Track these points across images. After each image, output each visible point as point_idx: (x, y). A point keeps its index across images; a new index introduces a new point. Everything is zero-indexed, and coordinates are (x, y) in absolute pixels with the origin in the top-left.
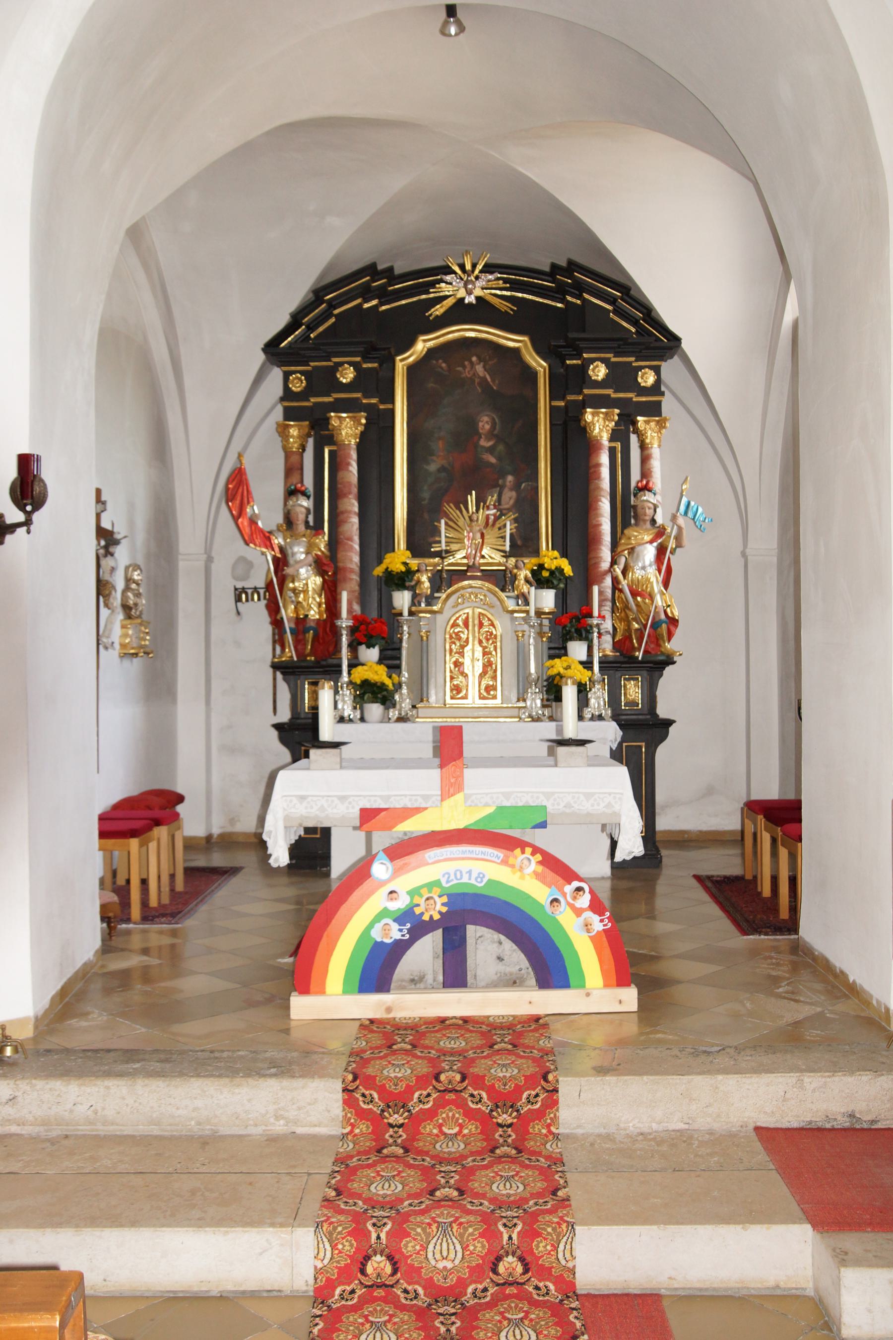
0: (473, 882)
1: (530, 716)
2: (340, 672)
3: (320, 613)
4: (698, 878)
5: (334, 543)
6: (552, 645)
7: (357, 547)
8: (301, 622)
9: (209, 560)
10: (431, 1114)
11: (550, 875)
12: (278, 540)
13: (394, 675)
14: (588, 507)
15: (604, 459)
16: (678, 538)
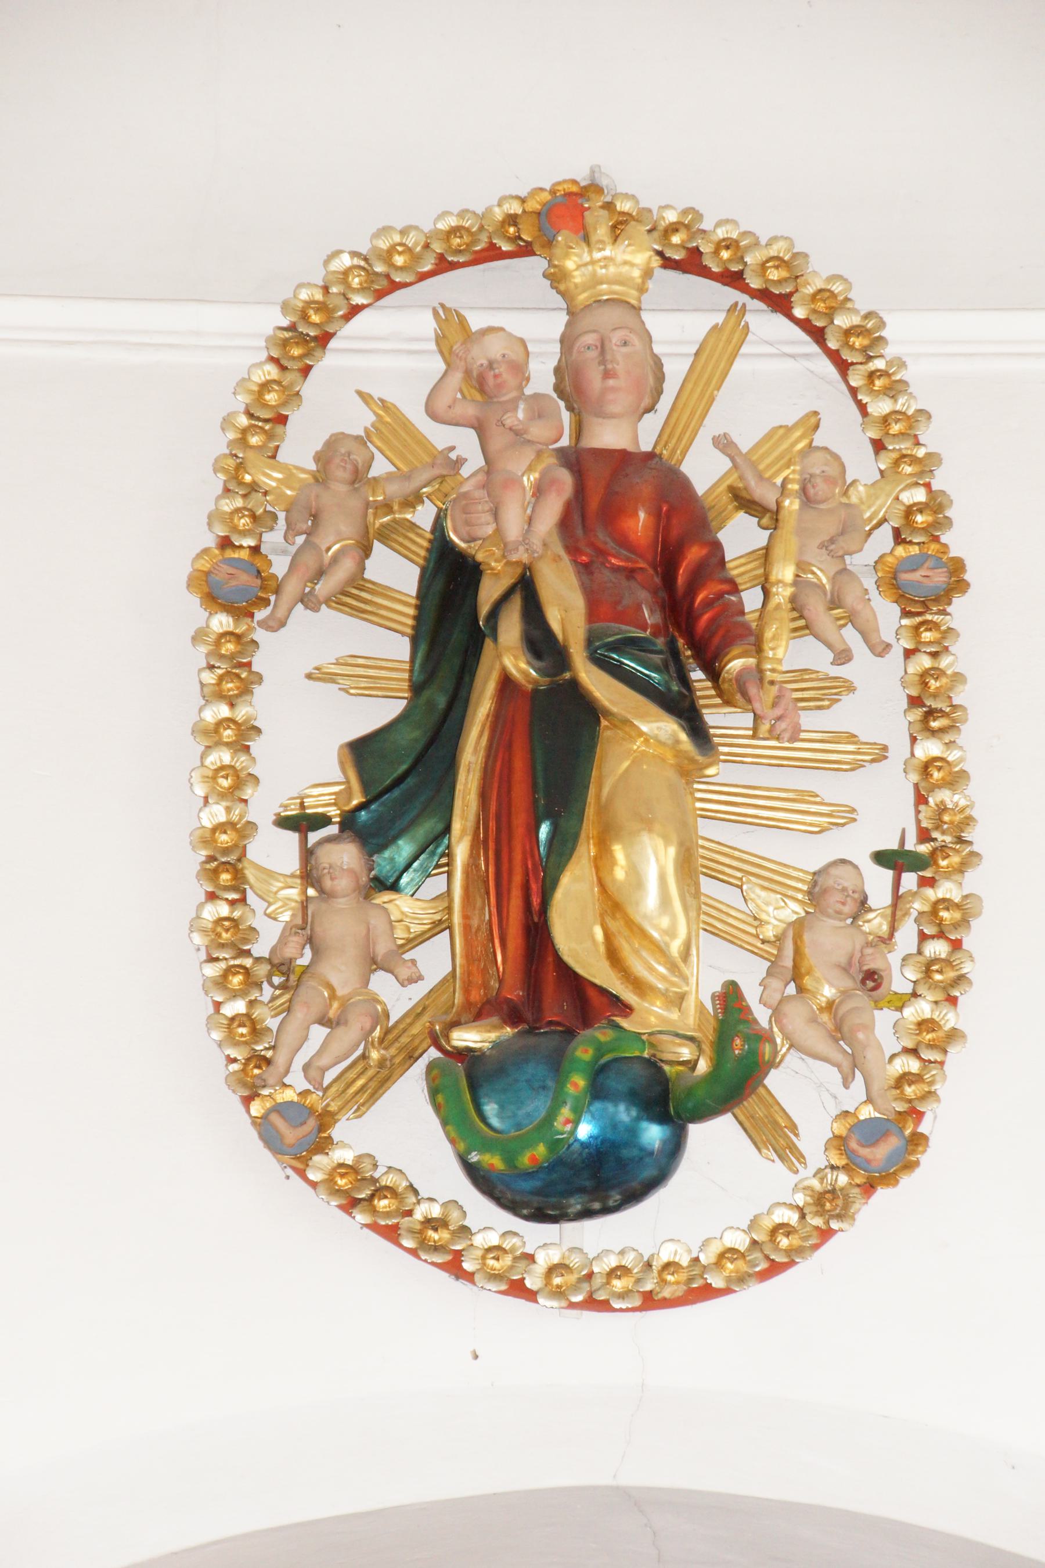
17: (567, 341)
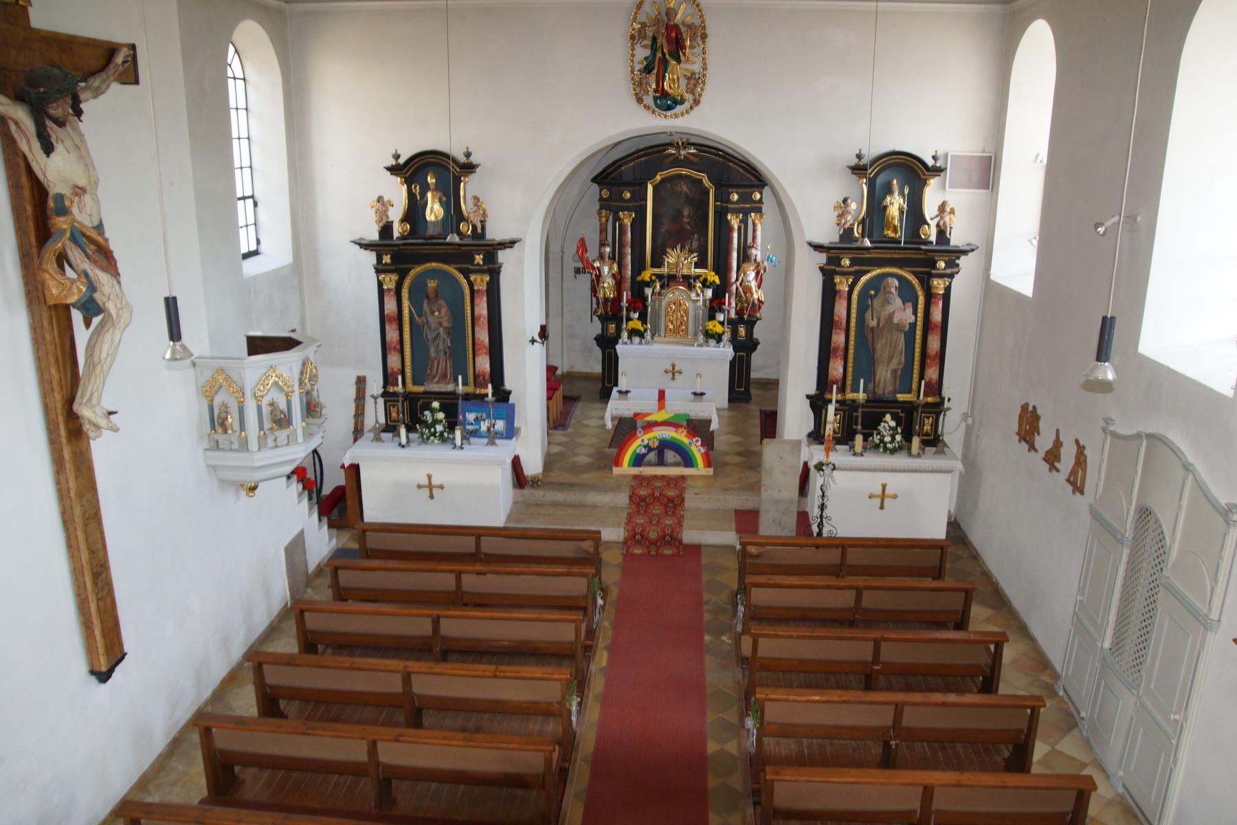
5: (620, 266)
7: (630, 268)
8: (606, 300)
15: (735, 235)
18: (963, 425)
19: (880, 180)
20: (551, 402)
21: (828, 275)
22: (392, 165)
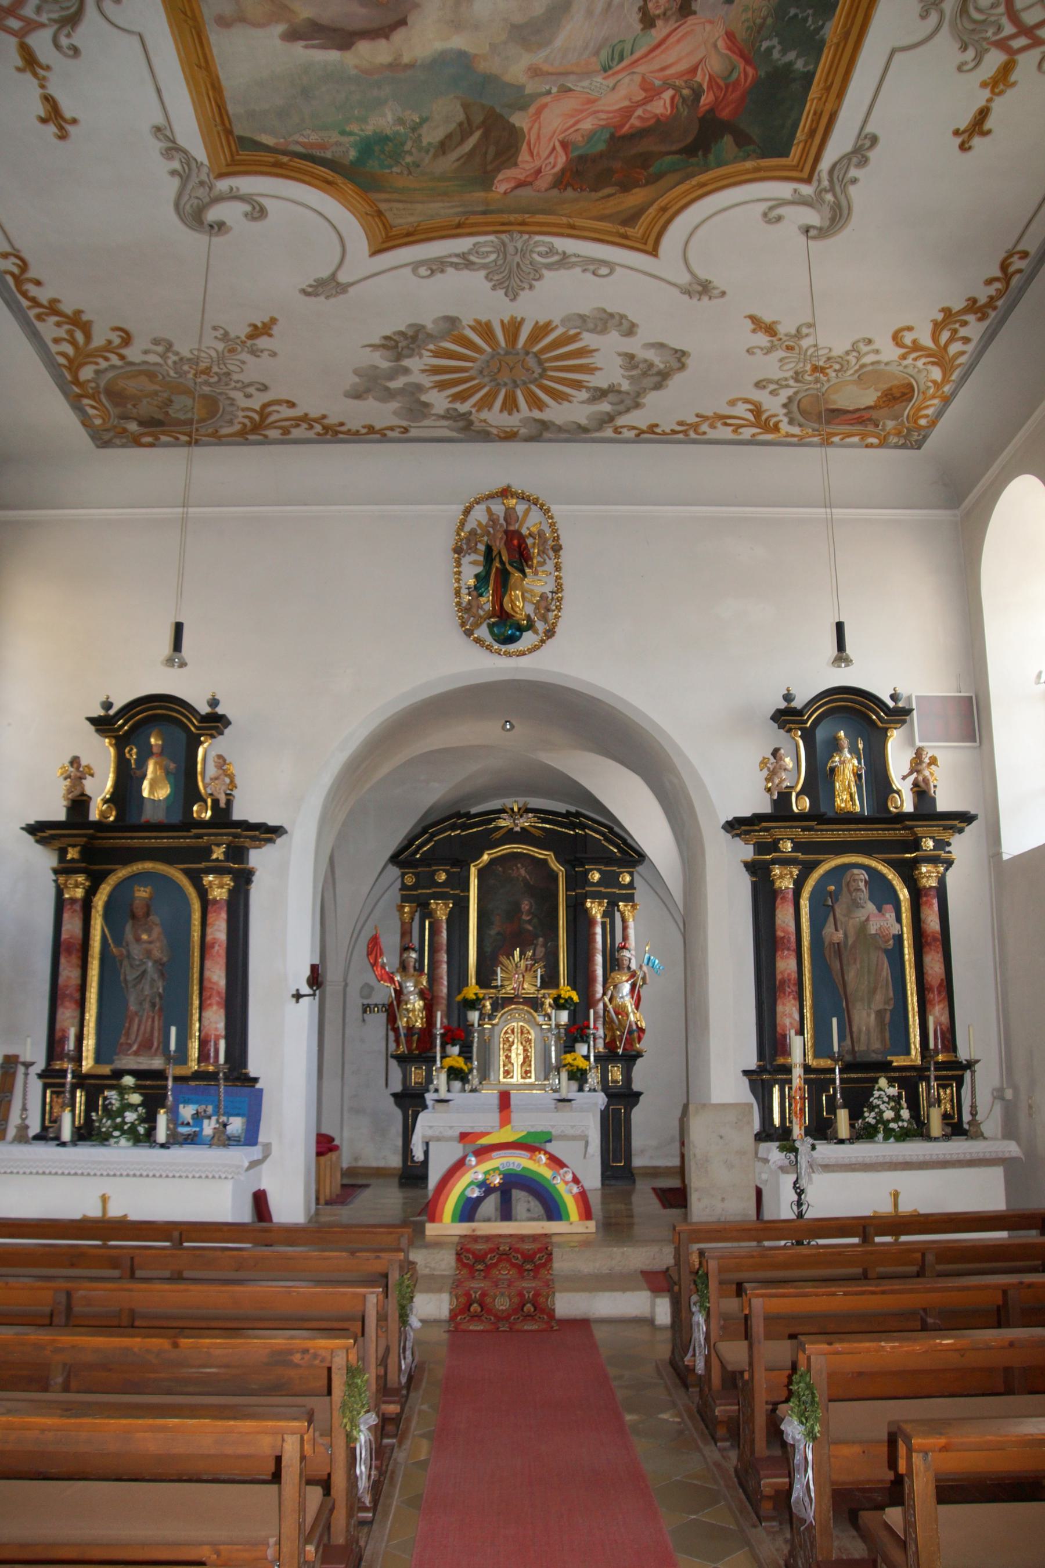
0: (515, 1168)
1: (552, 1089)
2: (435, 1061)
3: (422, 1023)
4: (654, 1189)
5: (433, 979)
6: (567, 1045)
7: (445, 983)
8: (410, 1029)
9: (346, 985)
10: (495, 1265)
11: (553, 1164)
12: (397, 978)
13: (469, 1064)
14: (590, 959)
15: (598, 930)
16: (644, 979)
17: (505, 514)
18: (998, 1108)
19: (820, 734)
20: (322, 1158)
21: (758, 871)
22: (100, 716)
